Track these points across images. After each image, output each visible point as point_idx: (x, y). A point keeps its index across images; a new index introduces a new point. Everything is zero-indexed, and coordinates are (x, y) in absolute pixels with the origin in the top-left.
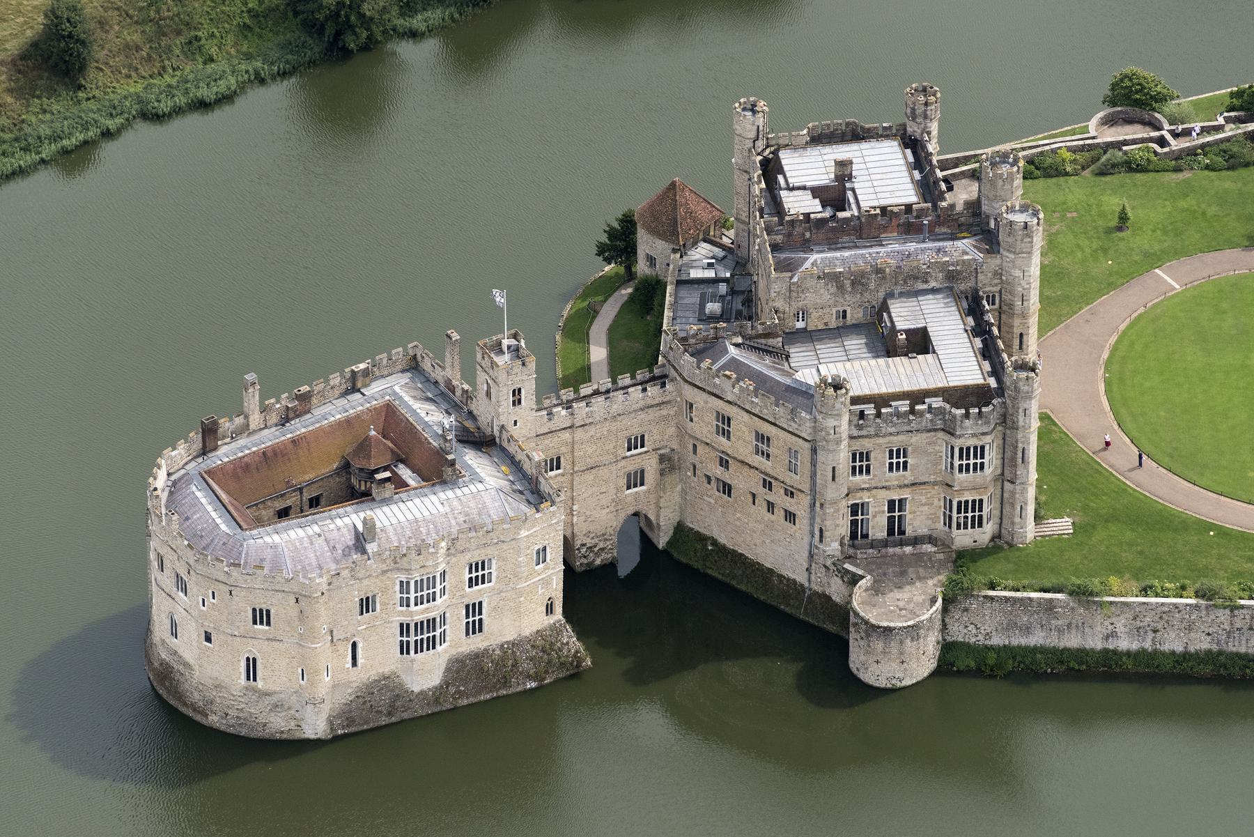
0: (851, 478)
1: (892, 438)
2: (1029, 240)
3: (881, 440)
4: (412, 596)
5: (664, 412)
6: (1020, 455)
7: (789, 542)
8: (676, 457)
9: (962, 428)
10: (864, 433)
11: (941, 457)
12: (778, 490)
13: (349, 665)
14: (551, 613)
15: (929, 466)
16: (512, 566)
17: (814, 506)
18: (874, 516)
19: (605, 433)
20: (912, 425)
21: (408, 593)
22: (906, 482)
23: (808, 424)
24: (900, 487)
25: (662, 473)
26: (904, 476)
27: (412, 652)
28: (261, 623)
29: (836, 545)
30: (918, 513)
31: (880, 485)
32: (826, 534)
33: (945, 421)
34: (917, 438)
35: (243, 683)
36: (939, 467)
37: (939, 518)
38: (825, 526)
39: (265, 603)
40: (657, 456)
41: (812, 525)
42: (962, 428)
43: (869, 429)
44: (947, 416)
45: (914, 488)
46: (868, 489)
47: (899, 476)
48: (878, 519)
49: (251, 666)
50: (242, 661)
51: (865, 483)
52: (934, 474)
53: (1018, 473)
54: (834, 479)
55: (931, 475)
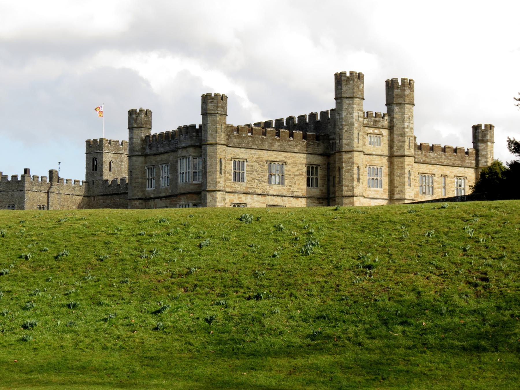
3: (158, 158)
20: (170, 146)
22: (168, 194)
46: (154, 198)
51: (152, 193)
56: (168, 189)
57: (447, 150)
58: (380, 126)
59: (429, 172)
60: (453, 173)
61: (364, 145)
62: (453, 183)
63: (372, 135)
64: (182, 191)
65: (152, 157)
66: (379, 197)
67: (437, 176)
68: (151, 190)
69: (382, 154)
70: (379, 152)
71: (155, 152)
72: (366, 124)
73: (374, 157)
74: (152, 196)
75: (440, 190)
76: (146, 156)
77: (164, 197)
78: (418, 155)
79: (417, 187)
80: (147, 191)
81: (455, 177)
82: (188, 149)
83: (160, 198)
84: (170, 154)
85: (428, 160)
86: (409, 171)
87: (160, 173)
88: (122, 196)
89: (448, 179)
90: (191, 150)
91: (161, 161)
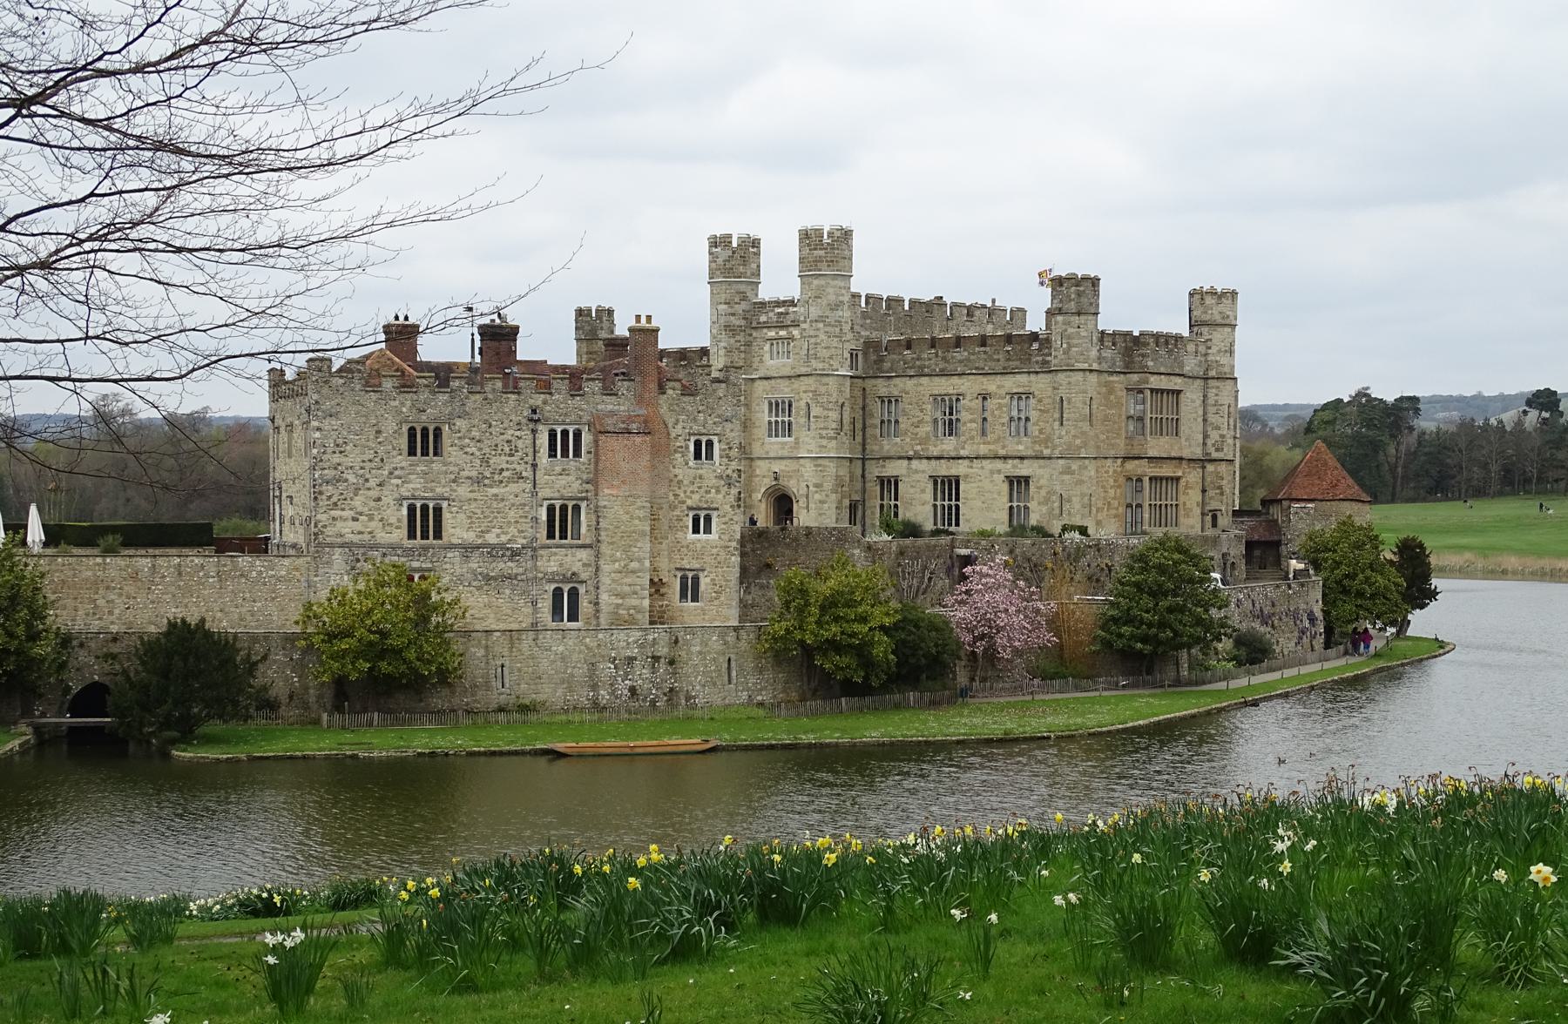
57: (989, 342)
58: (789, 323)
59: (951, 392)
60: (1003, 386)
61: (761, 361)
62: (1005, 409)
63: (775, 342)
66: (785, 453)
67: (968, 397)
69: (792, 374)
70: (787, 371)
72: (764, 322)
73: (779, 381)
75: (974, 425)
78: (930, 359)
79: (927, 422)
81: (1008, 397)
85: (950, 367)
86: (808, 405)
89: (991, 404)
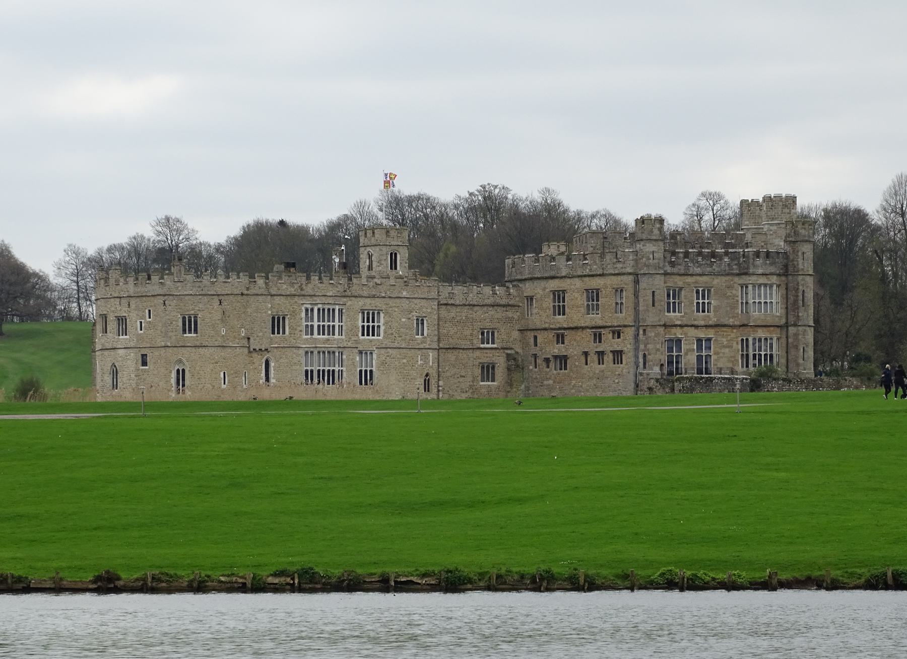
0: (666, 314)
1: (698, 278)
2: (788, 211)
3: (689, 279)
4: (316, 324)
5: (510, 314)
6: (801, 297)
7: (618, 383)
8: (520, 359)
9: (754, 266)
10: (675, 270)
11: (738, 301)
12: (607, 335)
13: (262, 381)
14: (428, 391)
15: (728, 309)
16: (397, 324)
17: (638, 335)
18: (686, 354)
19: (464, 318)
20: (714, 267)
21: (312, 320)
22: (710, 323)
23: (631, 257)
24: (706, 326)
25: (509, 369)
26: (708, 316)
27: (316, 380)
28: (190, 332)
29: (657, 369)
30: (721, 355)
31: (689, 323)
32: (649, 357)
33: (739, 265)
34: (718, 281)
35: (173, 396)
36: (736, 312)
37: (738, 361)
38: (648, 350)
39: (193, 309)
40: (505, 355)
41: (637, 357)
42: (754, 266)
43: (679, 267)
44: (741, 259)
45: (717, 329)
46: (681, 326)
47: (705, 316)
48: (689, 357)
49: (181, 376)
50: (173, 372)
51: (678, 319)
52: (733, 317)
53: (800, 314)
54: (653, 305)
55: (730, 318)
56: (711, 317)
64: (759, 323)
65: (678, 278)
68: (676, 316)
71: (682, 272)
74: (678, 323)
76: (666, 274)
77: (706, 326)
80: (667, 316)
82: (769, 276)
83: (696, 327)
84: (712, 277)
87: (693, 297)
88: (444, 307)
90: (775, 277)
91: (696, 282)
